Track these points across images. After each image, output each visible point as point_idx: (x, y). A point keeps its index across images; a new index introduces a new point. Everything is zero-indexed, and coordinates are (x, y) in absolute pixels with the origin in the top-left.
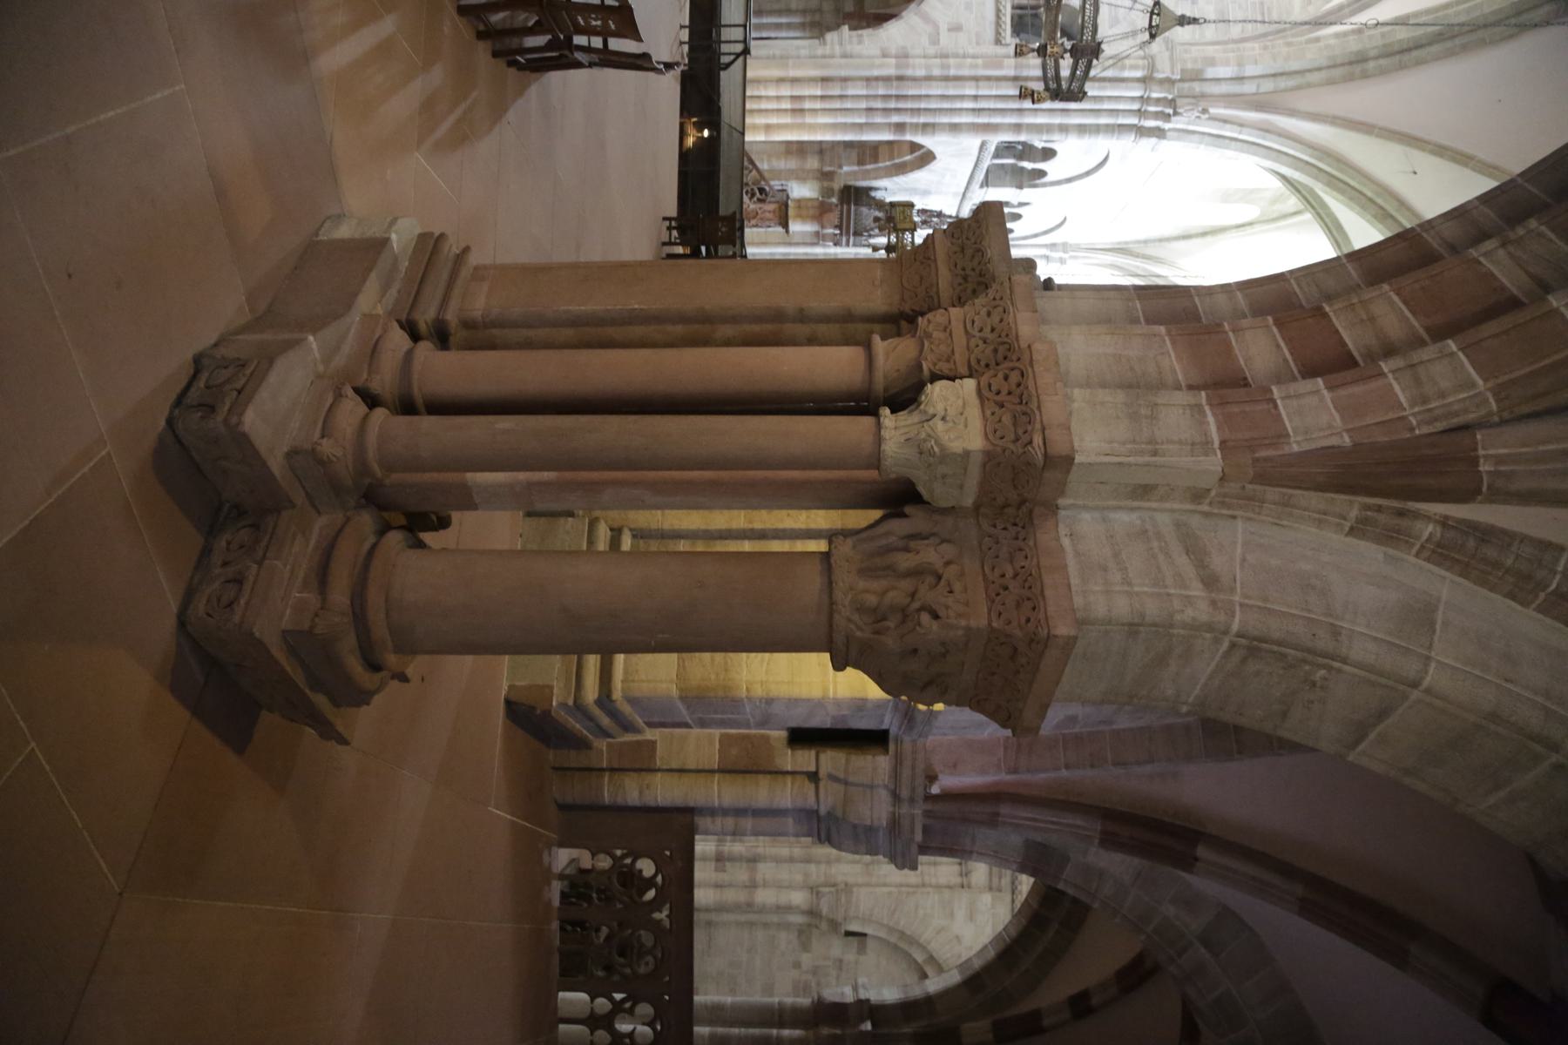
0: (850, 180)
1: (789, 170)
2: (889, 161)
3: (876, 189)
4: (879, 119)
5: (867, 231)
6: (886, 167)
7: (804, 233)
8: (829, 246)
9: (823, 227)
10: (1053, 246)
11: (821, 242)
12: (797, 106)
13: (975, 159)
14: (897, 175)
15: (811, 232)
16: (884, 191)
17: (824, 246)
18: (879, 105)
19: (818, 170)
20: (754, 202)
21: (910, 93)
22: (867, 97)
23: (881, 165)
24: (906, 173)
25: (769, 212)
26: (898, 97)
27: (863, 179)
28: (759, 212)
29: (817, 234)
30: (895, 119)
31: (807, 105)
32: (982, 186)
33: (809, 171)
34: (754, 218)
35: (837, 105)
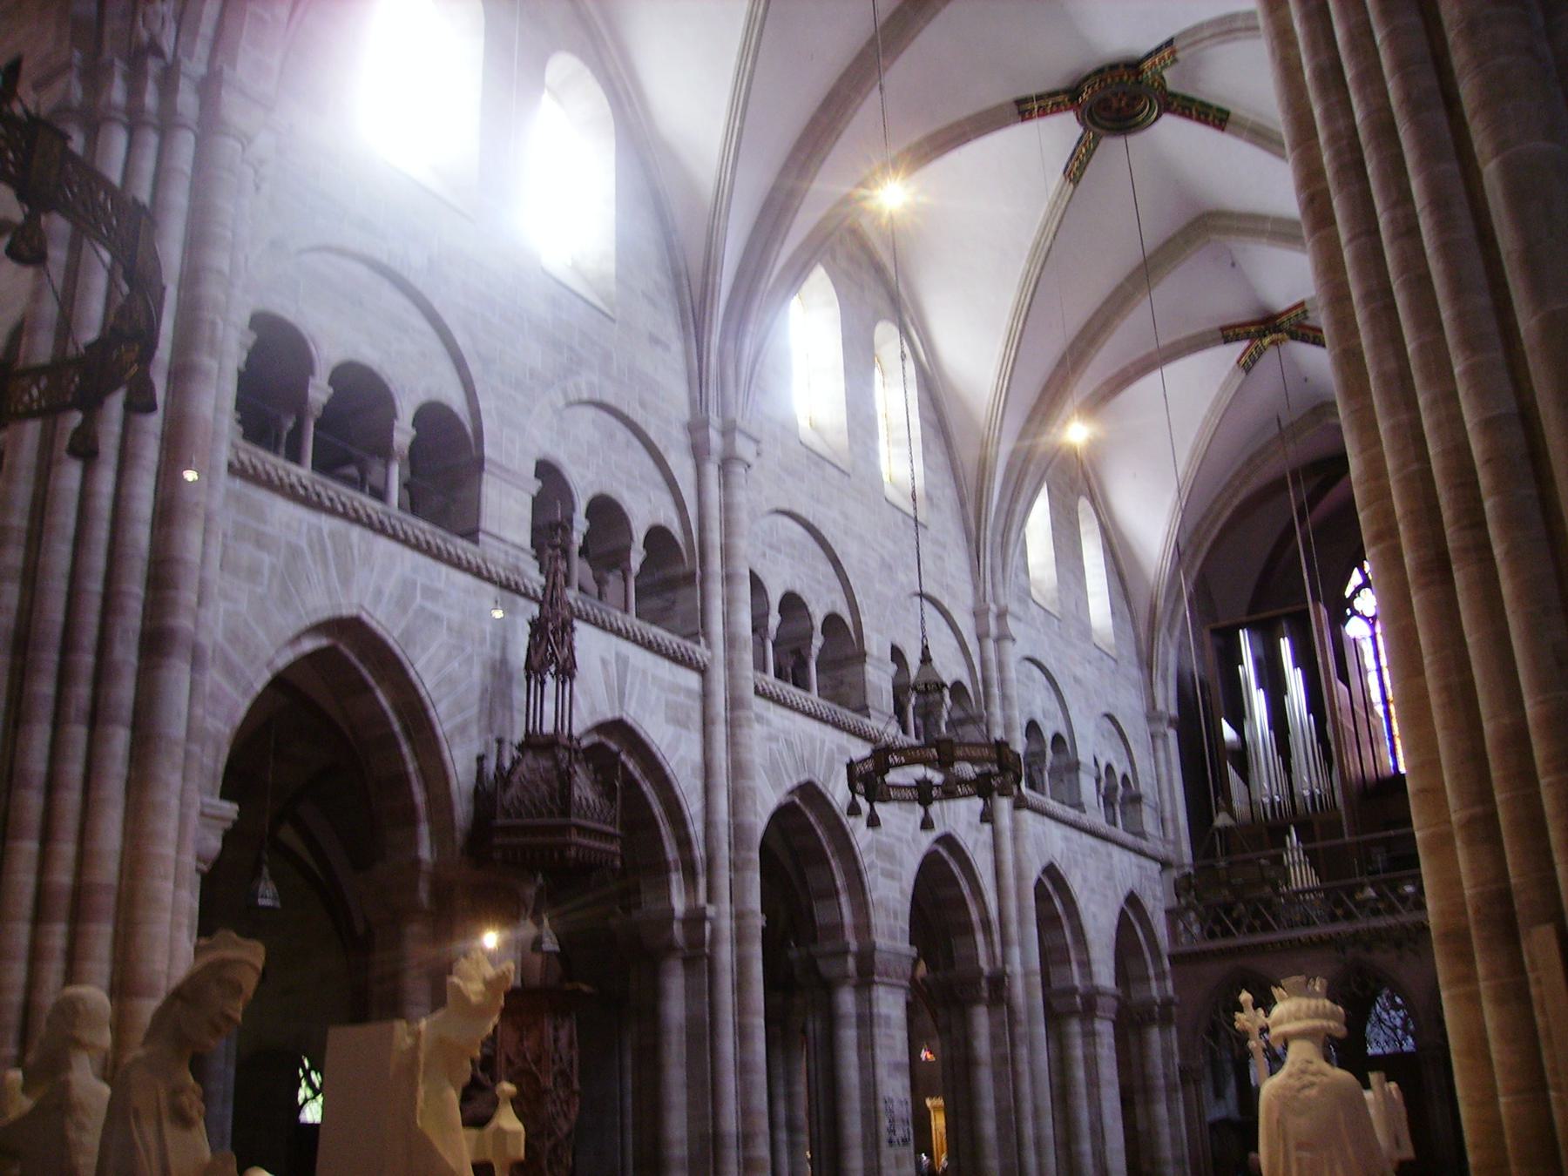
4: (125, 691)
7: (691, 993)
8: (714, 931)
9: (671, 948)
10: (699, 452)
12: (62, 905)
13: (356, 533)
14: (432, 728)
16: (485, 762)
18: (82, 692)
21: (59, 617)
22: (59, 722)
24: (420, 700)
26: (68, 644)
29: (690, 962)
30: (127, 653)
31: (63, 877)
32: (476, 542)
35: (71, 799)
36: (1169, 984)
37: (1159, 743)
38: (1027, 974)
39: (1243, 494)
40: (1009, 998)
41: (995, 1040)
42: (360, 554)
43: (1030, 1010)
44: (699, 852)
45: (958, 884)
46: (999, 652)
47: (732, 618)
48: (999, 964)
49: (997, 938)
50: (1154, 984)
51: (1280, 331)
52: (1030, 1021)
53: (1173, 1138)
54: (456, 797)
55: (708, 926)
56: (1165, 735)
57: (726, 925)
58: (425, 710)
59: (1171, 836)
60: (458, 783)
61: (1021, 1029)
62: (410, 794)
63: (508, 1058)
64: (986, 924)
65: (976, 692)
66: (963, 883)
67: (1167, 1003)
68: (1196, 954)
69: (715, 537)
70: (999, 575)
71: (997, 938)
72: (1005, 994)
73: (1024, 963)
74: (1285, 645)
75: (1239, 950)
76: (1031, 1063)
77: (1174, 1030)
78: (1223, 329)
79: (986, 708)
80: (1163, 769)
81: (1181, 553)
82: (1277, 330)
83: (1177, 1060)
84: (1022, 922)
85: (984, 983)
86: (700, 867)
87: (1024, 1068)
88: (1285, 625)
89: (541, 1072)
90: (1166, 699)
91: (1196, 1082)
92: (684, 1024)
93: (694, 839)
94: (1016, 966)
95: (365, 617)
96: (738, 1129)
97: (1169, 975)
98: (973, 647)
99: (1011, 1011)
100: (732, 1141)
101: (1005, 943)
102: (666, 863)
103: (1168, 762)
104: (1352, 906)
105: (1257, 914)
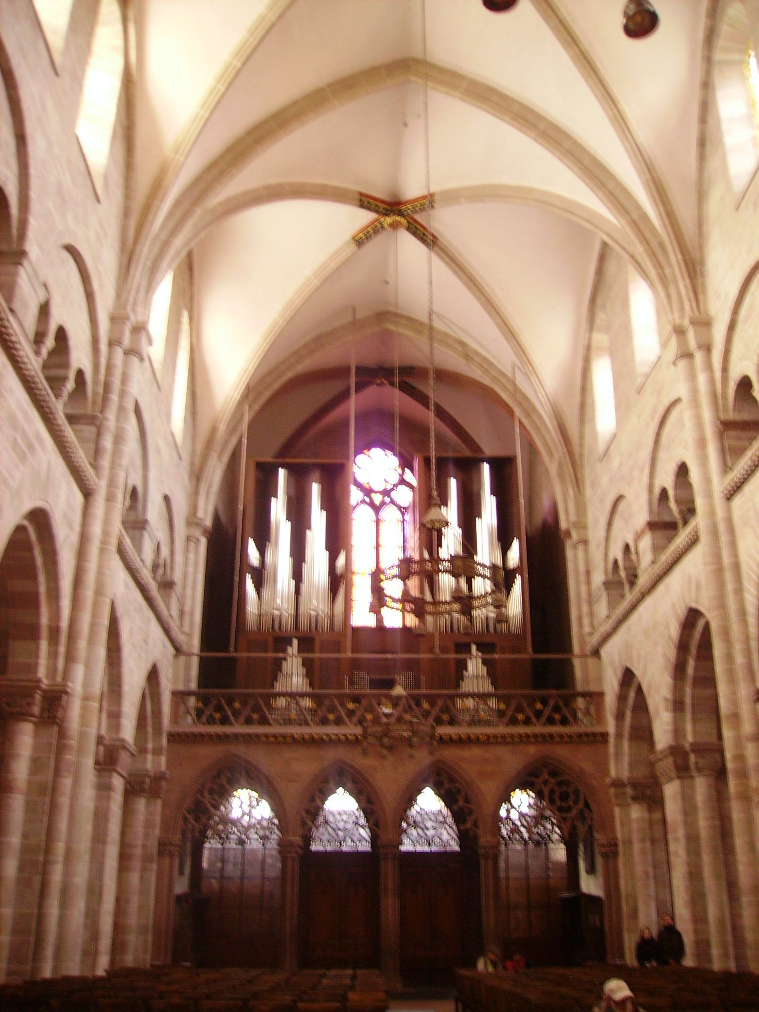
36: (163, 760)
37: (192, 544)
38: (86, 698)
39: (301, 368)
40: (63, 720)
41: (36, 764)
43: (83, 736)
45: (35, 577)
46: (126, 364)
48: (59, 679)
49: (62, 649)
50: (150, 757)
51: (403, 216)
52: (80, 751)
53: (141, 908)
56: (198, 540)
59: (186, 629)
61: (69, 757)
64: (55, 632)
65: (95, 393)
66: (42, 578)
67: (159, 778)
68: (194, 735)
70: (142, 295)
71: (62, 649)
72: (60, 714)
73: (86, 685)
74: (316, 489)
75: (236, 736)
76: (74, 797)
77: (159, 803)
78: (361, 194)
79: (102, 412)
80: (191, 569)
81: (250, 392)
82: (401, 214)
83: (157, 832)
84: (91, 641)
85: (38, 697)
87: (64, 801)
88: (316, 474)
90: (206, 510)
91: (171, 855)
94: (77, 685)
97: (165, 752)
98: (103, 347)
99: (62, 734)
101: (70, 658)
103: (196, 564)
104: (343, 713)
105: (257, 709)
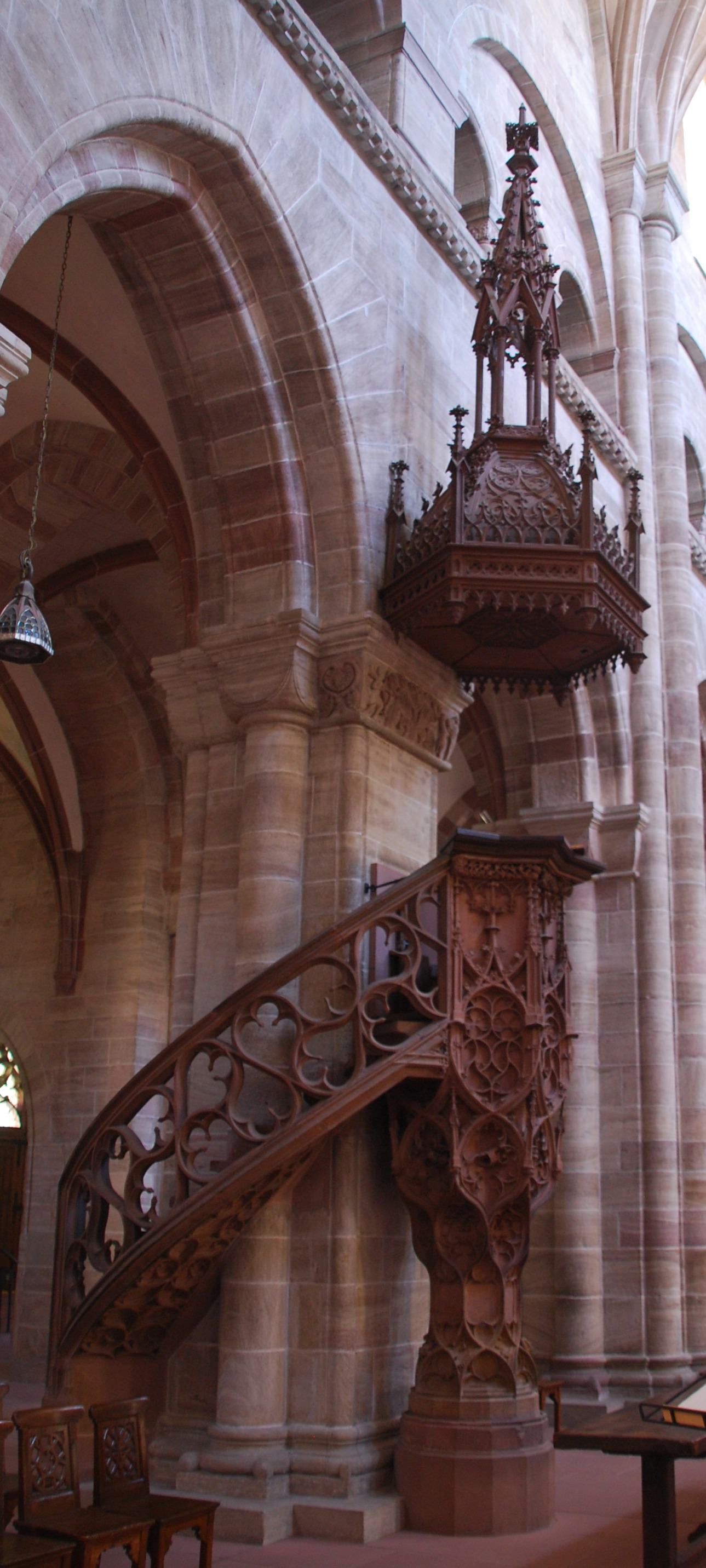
0: (355, 588)
1: (306, 854)
2: (269, 420)
3: (396, 499)
5: (569, 500)
6: (299, 444)
8: (646, 844)
11: (635, 871)
14: (330, 393)
15: (599, 910)
17: (646, 860)
19: (312, 732)
20: (439, 1001)
23: (288, 458)
24: (315, 337)
25: (487, 933)
27: (351, 538)
28: (485, 980)
29: (603, 889)
33: (314, 775)
34: (518, 1012)
42: (242, 48)
44: (624, 729)
47: (661, 419)
54: (361, 517)
55: (638, 835)
57: (662, 838)
58: (321, 360)
60: (365, 493)
62: (284, 506)
63: (465, 963)
69: (637, 309)
86: (626, 751)
89: (524, 994)
92: (595, 976)
93: (619, 707)
95: (244, 153)
96: (678, 1139)
100: (672, 1154)
102: (579, 739)
